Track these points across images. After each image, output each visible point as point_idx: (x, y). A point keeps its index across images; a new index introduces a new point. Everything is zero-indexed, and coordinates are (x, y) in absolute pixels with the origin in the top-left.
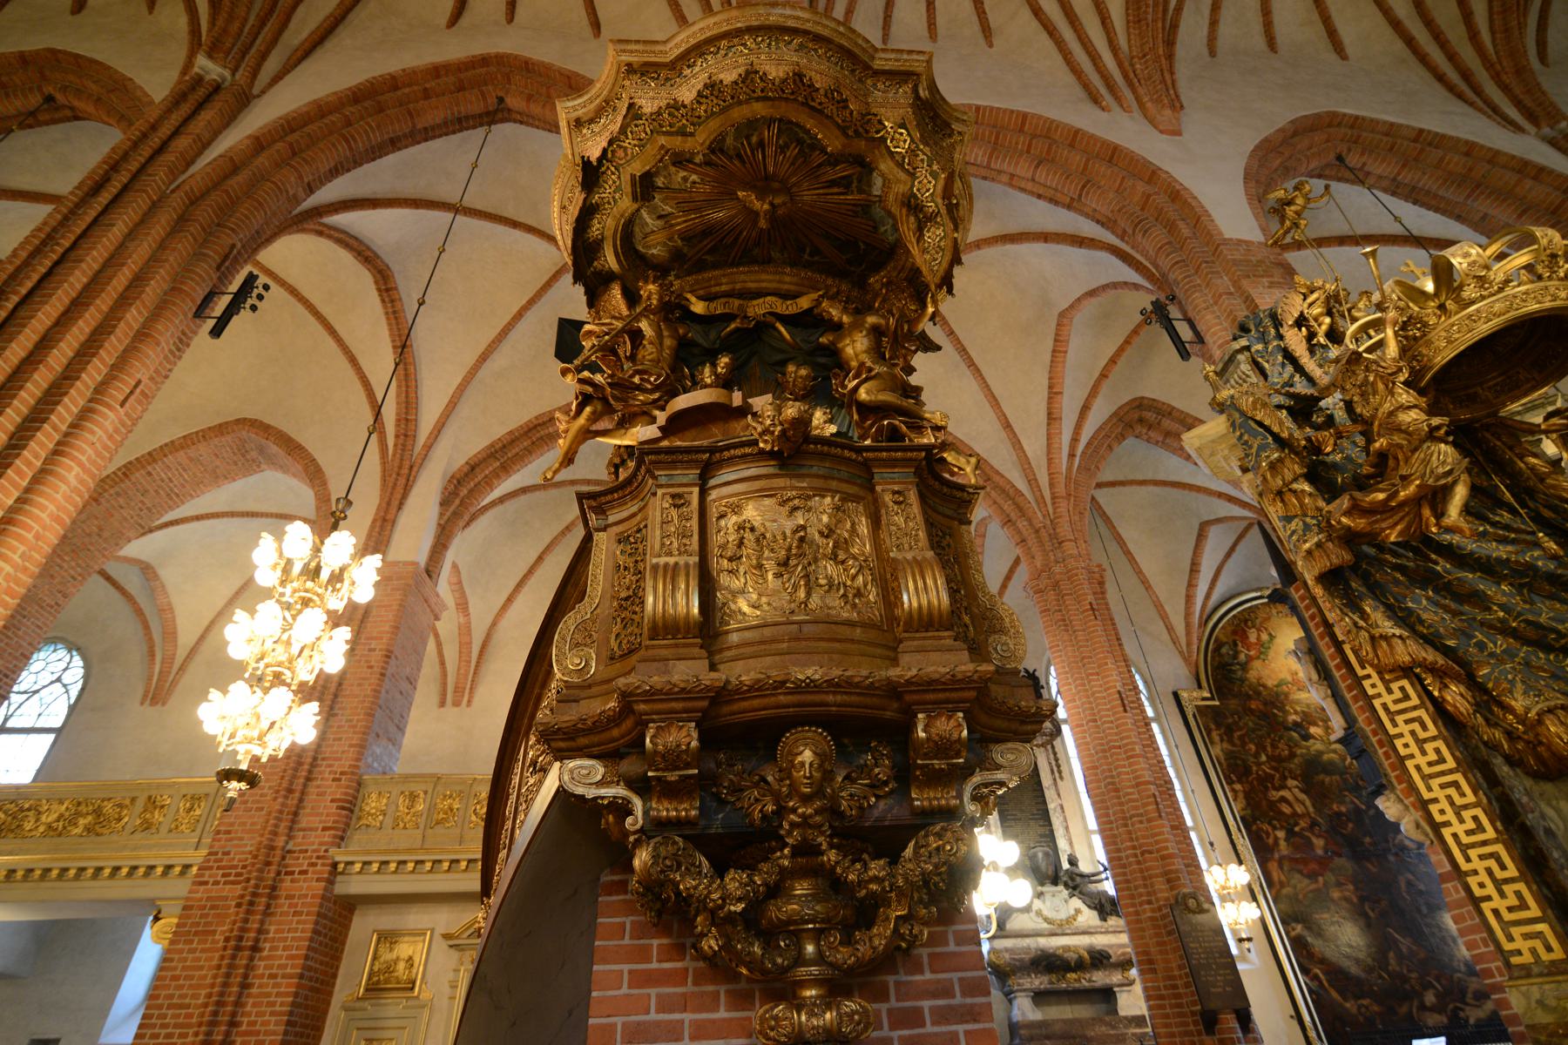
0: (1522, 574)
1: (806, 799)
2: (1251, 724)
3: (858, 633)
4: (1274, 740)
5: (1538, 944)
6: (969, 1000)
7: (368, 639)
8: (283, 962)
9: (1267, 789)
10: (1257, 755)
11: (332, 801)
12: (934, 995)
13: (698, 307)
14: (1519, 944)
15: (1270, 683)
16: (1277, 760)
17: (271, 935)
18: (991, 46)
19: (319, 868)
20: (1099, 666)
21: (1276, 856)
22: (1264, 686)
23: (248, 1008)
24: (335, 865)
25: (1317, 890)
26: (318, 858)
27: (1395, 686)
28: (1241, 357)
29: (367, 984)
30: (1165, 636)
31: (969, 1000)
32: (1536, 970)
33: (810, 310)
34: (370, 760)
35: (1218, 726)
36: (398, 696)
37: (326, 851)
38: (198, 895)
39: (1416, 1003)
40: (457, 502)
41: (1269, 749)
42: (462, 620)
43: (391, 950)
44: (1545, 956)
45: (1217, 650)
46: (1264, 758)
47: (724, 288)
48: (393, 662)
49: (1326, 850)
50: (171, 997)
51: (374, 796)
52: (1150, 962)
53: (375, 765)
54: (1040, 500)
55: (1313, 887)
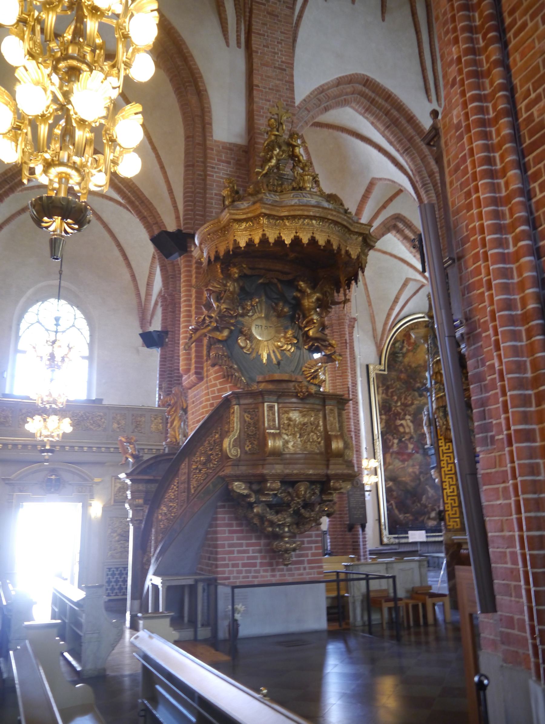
2: (398, 386)
3: (318, 457)
4: (406, 395)
9: (396, 419)
10: (396, 402)
14: (451, 523)
15: (413, 365)
16: (405, 405)
18: (383, 20)
20: (343, 373)
21: (391, 450)
22: (410, 366)
25: (404, 467)
27: (448, 444)
30: (371, 333)
35: (383, 385)
39: (427, 516)
41: (403, 399)
45: (394, 344)
46: (399, 404)
47: (261, 266)
49: (413, 450)
55: (402, 466)
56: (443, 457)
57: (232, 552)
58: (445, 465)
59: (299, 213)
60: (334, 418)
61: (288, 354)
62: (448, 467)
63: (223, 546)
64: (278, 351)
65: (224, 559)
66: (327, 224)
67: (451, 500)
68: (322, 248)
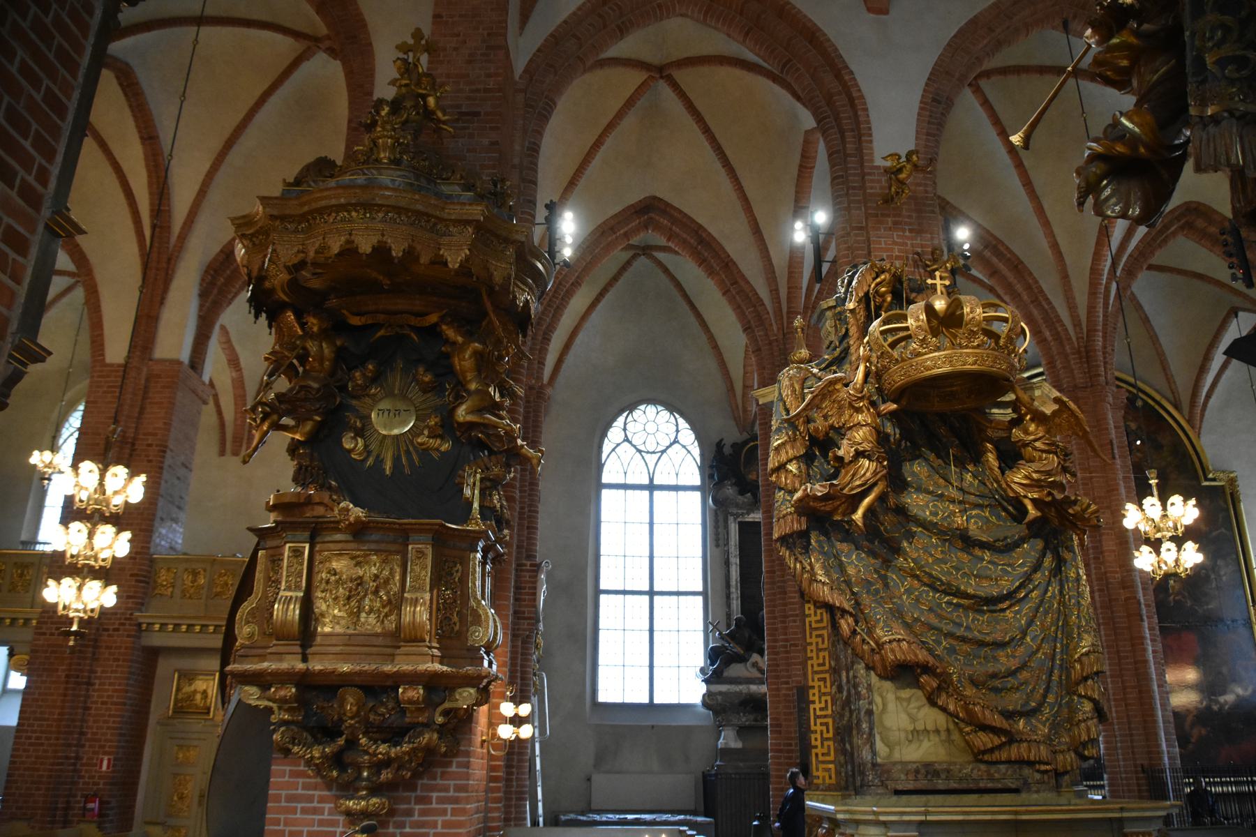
0: (945, 533)
1: (352, 718)
3: (380, 641)
5: (827, 775)
6: (457, 794)
7: (145, 434)
8: (110, 693)
11: (132, 575)
12: (440, 791)
13: (355, 321)
14: (820, 774)
17: (99, 674)
19: (127, 627)
23: (90, 724)
24: (140, 625)
26: (126, 619)
27: (819, 611)
28: (829, 314)
29: (174, 708)
31: (457, 794)
32: (821, 787)
33: (436, 325)
34: (158, 540)
36: (176, 482)
37: (131, 614)
38: (41, 642)
40: (215, 291)
42: (234, 374)
43: (190, 685)
44: (827, 781)
48: (169, 454)
50: (34, 712)
51: (163, 572)
52: (779, 725)
53: (163, 543)
54: (778, 310)
56: (811, 637)
57: (294, 811)
58: (814, 655)
59: (323, 203)
60: (424, 568)
61: (435, 455)
62: (818, 658)
63: (277, 799)
64: (417, 451)
65: (277, 822)
66: (381, 215)
67: (822, 724)
68: (364, 257)
